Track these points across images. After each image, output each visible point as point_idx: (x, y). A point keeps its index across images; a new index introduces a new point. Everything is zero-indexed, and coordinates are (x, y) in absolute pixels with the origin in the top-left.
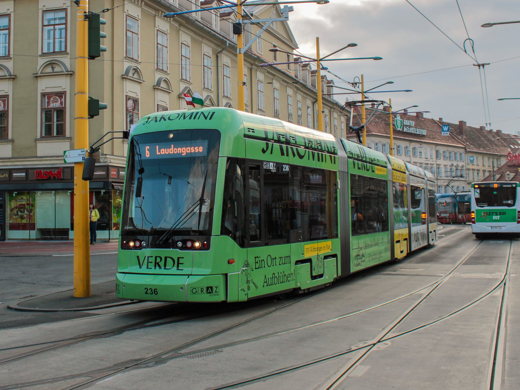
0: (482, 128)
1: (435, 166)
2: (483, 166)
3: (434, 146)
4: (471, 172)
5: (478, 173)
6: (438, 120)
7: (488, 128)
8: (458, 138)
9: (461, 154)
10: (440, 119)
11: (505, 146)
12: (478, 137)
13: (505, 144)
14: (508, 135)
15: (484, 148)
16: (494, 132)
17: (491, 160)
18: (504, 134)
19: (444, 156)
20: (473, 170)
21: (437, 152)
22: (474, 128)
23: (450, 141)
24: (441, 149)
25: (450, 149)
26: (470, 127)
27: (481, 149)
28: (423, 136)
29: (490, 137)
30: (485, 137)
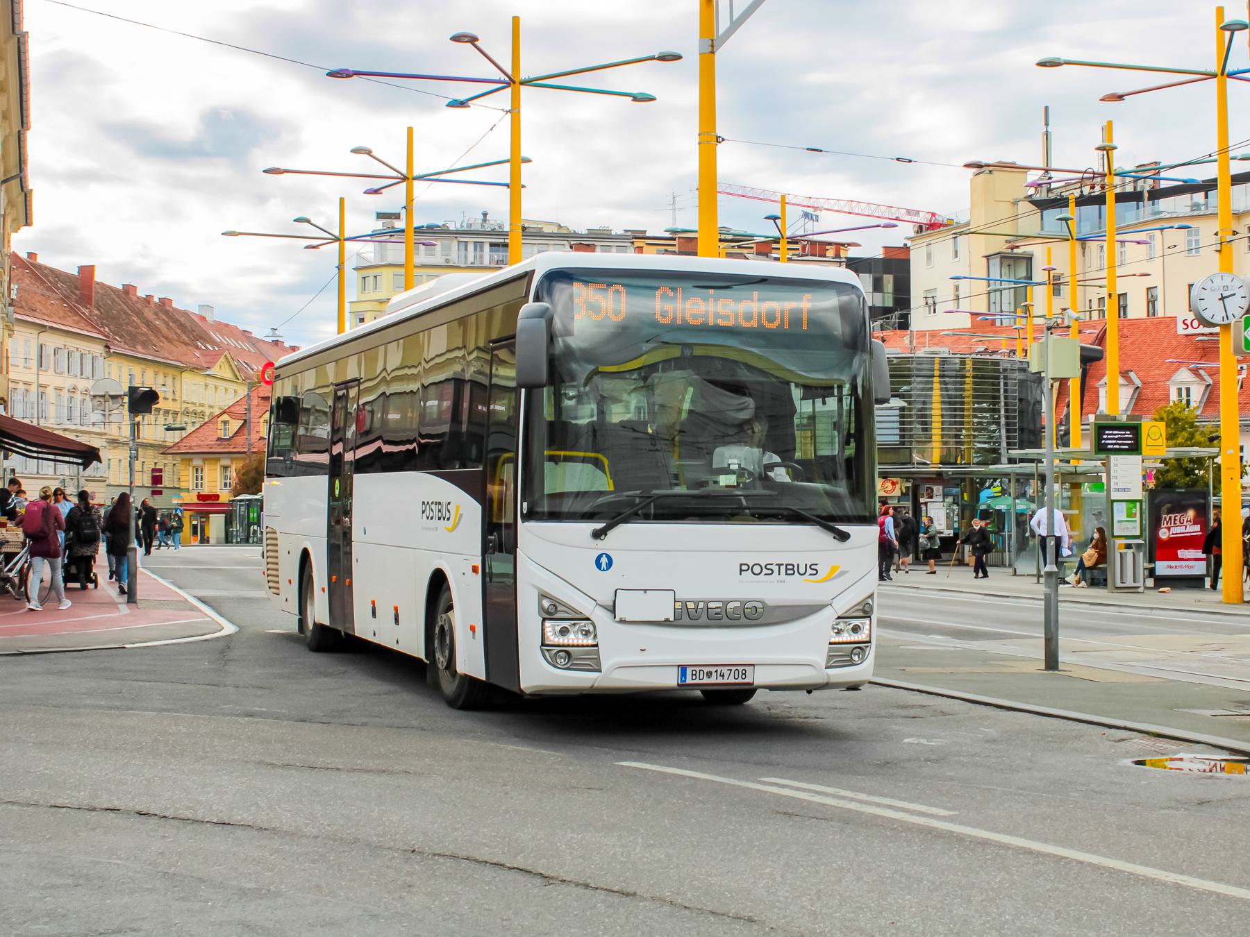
0: (128, 290)
1: (34, 388)
7: (141, 293)
10: (31, 255)
11: (186, 344)
12: (125, 313)
13: (184, 337)
14: (185, 314)
15: (144, 344)
18: (175, 310)
19: (56, 362)
23: (70, 321)
24: (52, 341)
25: (73, 343)
26: (102, 285)
27: (139, 348)
29: (149, 314)
30: (139, 314)
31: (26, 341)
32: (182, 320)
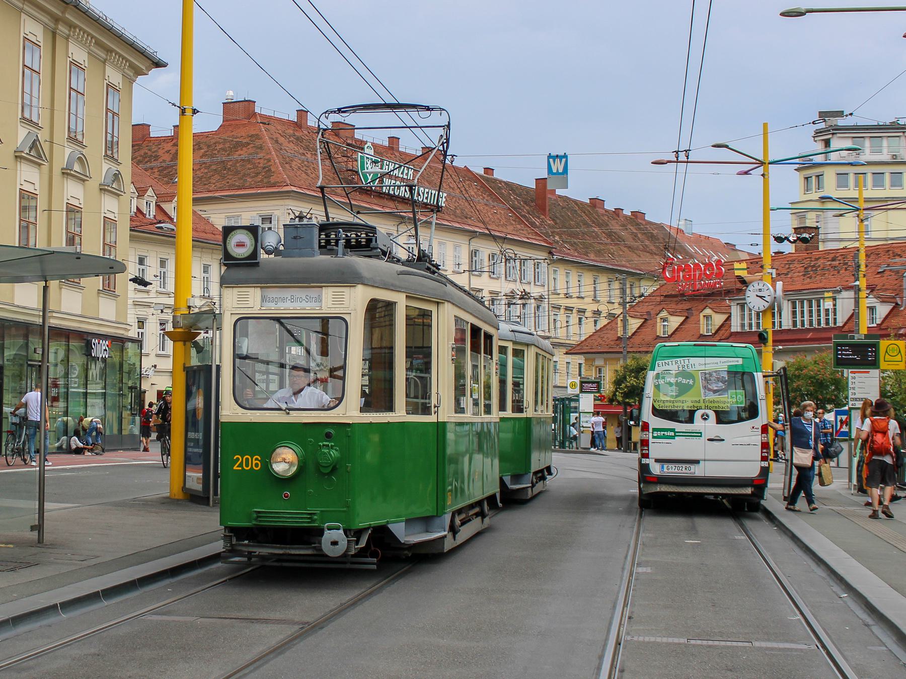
0: (596, 203)
2: (595, 300)
3: (462, 240)
4: (562, 311)
5: (580, 319)
6: (482, 172)
7: (610, 206)
8: (533, 224)
9: (537, 266)
12: (586, 224)
15: (599, 253)
16: (626, 217)
17: (616, 285)
20: (569, 309)
21: (474, 254)
22: (575, 202)
23: (510, 229)
24: (486, 249)
25: (511, 250)
27: (592, 256)
28: (437, 209)
29: (615, 227)
31: (456, 247)
32: (655, 232)
